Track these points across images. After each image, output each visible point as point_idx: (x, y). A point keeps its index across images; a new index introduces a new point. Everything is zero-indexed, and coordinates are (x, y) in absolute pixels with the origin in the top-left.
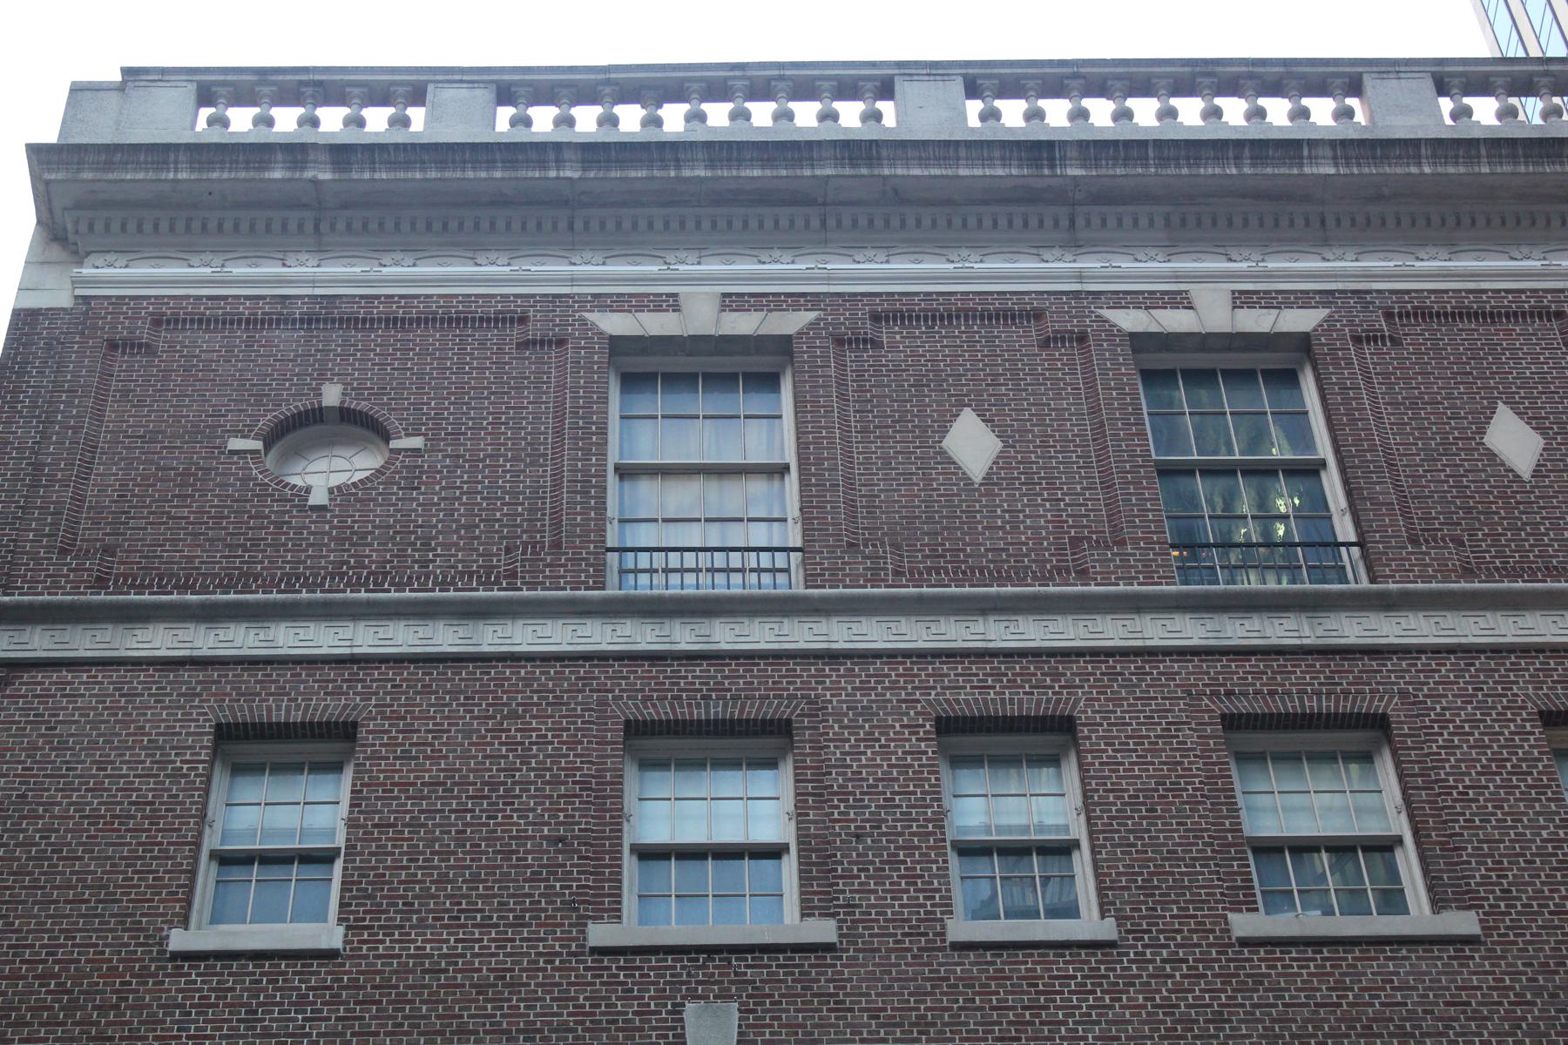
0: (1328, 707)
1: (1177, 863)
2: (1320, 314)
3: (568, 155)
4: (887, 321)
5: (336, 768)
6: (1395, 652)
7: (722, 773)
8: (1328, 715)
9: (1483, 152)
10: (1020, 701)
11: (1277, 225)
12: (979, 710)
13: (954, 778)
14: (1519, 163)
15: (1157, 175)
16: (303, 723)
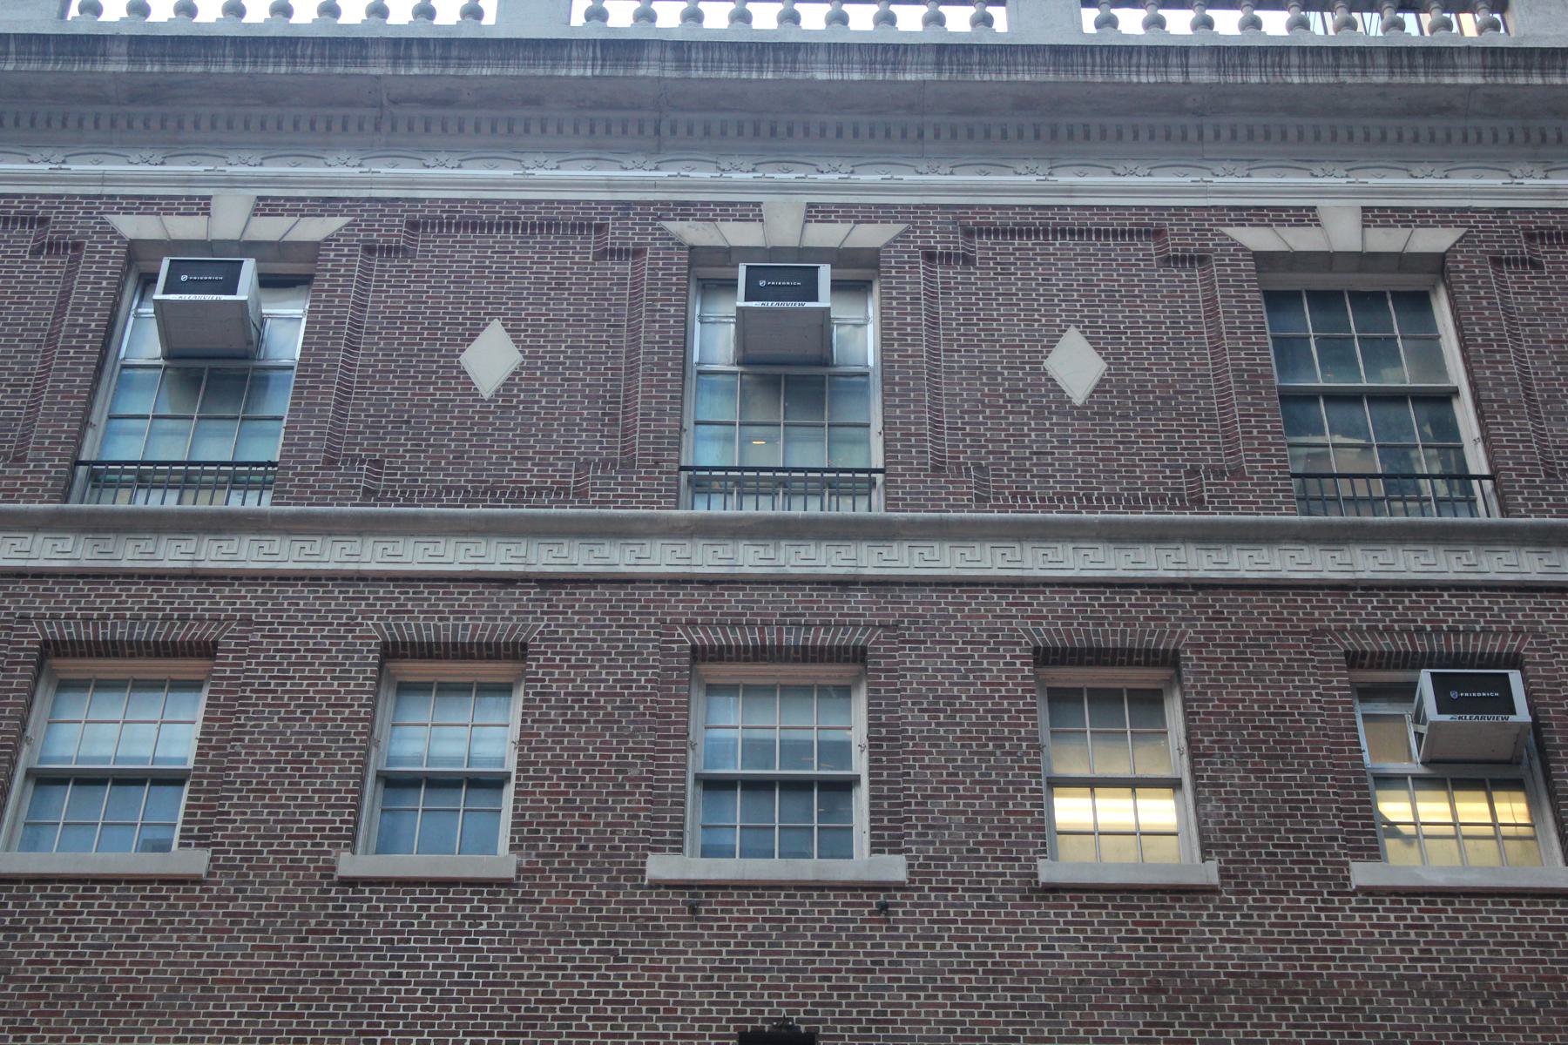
0: (754, 639)
1: (594, 799)
2: (894, 229)
3: (114, 48)
4: (425, 228)
5: (195, 686)
6: (749, 583)
7: (143, 694)
8: (755, 647)
9: (12, 48)
10: (495, 628)
11: (329, 128)
12: (392, 635)
13: (708, 708)
14: (48, 61)
15: (14, 71)
16: (147, 643)
